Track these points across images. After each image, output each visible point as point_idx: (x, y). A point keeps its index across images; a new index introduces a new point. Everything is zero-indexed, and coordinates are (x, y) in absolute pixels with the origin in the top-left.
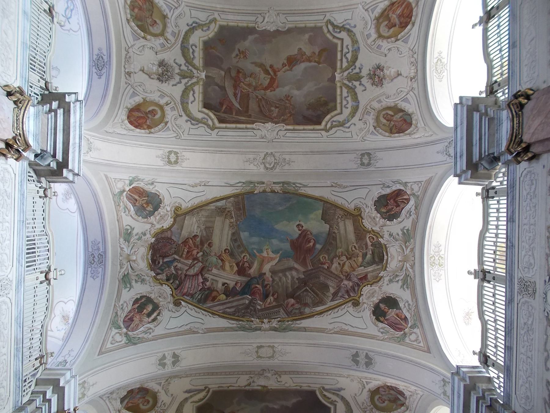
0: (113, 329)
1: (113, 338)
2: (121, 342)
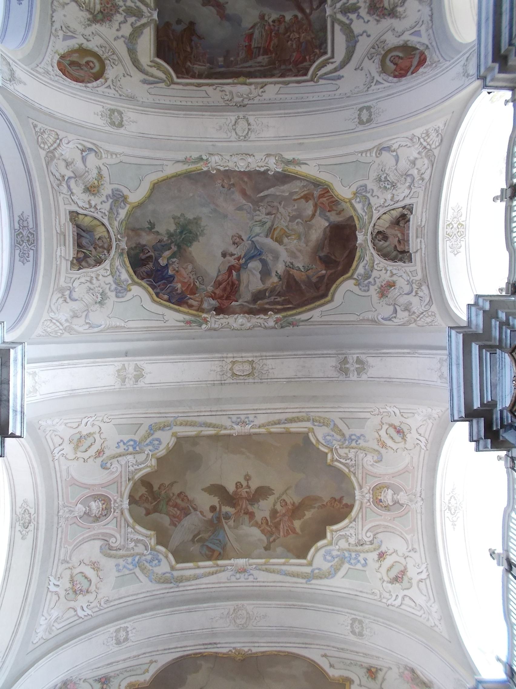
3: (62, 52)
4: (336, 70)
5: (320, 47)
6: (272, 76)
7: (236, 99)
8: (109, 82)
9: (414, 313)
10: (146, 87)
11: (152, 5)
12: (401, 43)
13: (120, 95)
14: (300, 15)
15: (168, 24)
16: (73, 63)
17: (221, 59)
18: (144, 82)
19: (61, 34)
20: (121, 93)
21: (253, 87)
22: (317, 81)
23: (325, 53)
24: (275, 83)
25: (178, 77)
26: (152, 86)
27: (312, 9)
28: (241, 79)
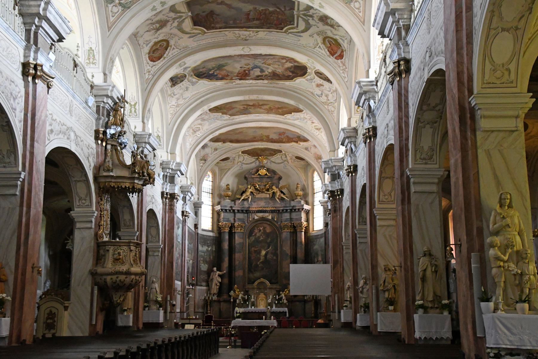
0: (109, 5)
1: (111, 11)
2: (118, 11)
3: (148, 51)
4: (298, 32)
5: (290, 22)
6: (262, 28)
7: (242, 37)
8: (173, 46)
9: (329, 100)
10: (192, 39)
11: (187, 11)
12: (335, 38)
13: (180, 50)
14: (278, 10)
15: (198, 15)
16: (154, 52)
17: (231, 22)
18: (190, 37)
19: (145, 45)
20: (180, 48)
21: (251, 32)
22: (288, 34)
23: (294, 25)
24: (264, 31)
25: (208, 30)
26: (195, 37)
27: (285, 10)
28: (244, 29)
